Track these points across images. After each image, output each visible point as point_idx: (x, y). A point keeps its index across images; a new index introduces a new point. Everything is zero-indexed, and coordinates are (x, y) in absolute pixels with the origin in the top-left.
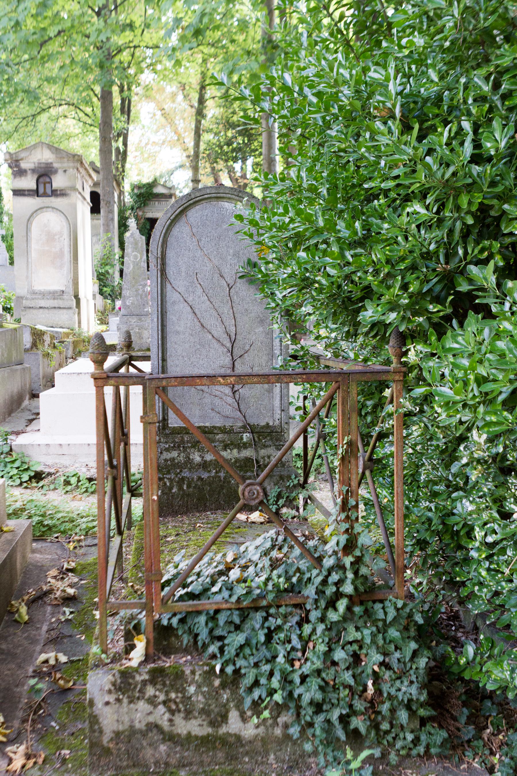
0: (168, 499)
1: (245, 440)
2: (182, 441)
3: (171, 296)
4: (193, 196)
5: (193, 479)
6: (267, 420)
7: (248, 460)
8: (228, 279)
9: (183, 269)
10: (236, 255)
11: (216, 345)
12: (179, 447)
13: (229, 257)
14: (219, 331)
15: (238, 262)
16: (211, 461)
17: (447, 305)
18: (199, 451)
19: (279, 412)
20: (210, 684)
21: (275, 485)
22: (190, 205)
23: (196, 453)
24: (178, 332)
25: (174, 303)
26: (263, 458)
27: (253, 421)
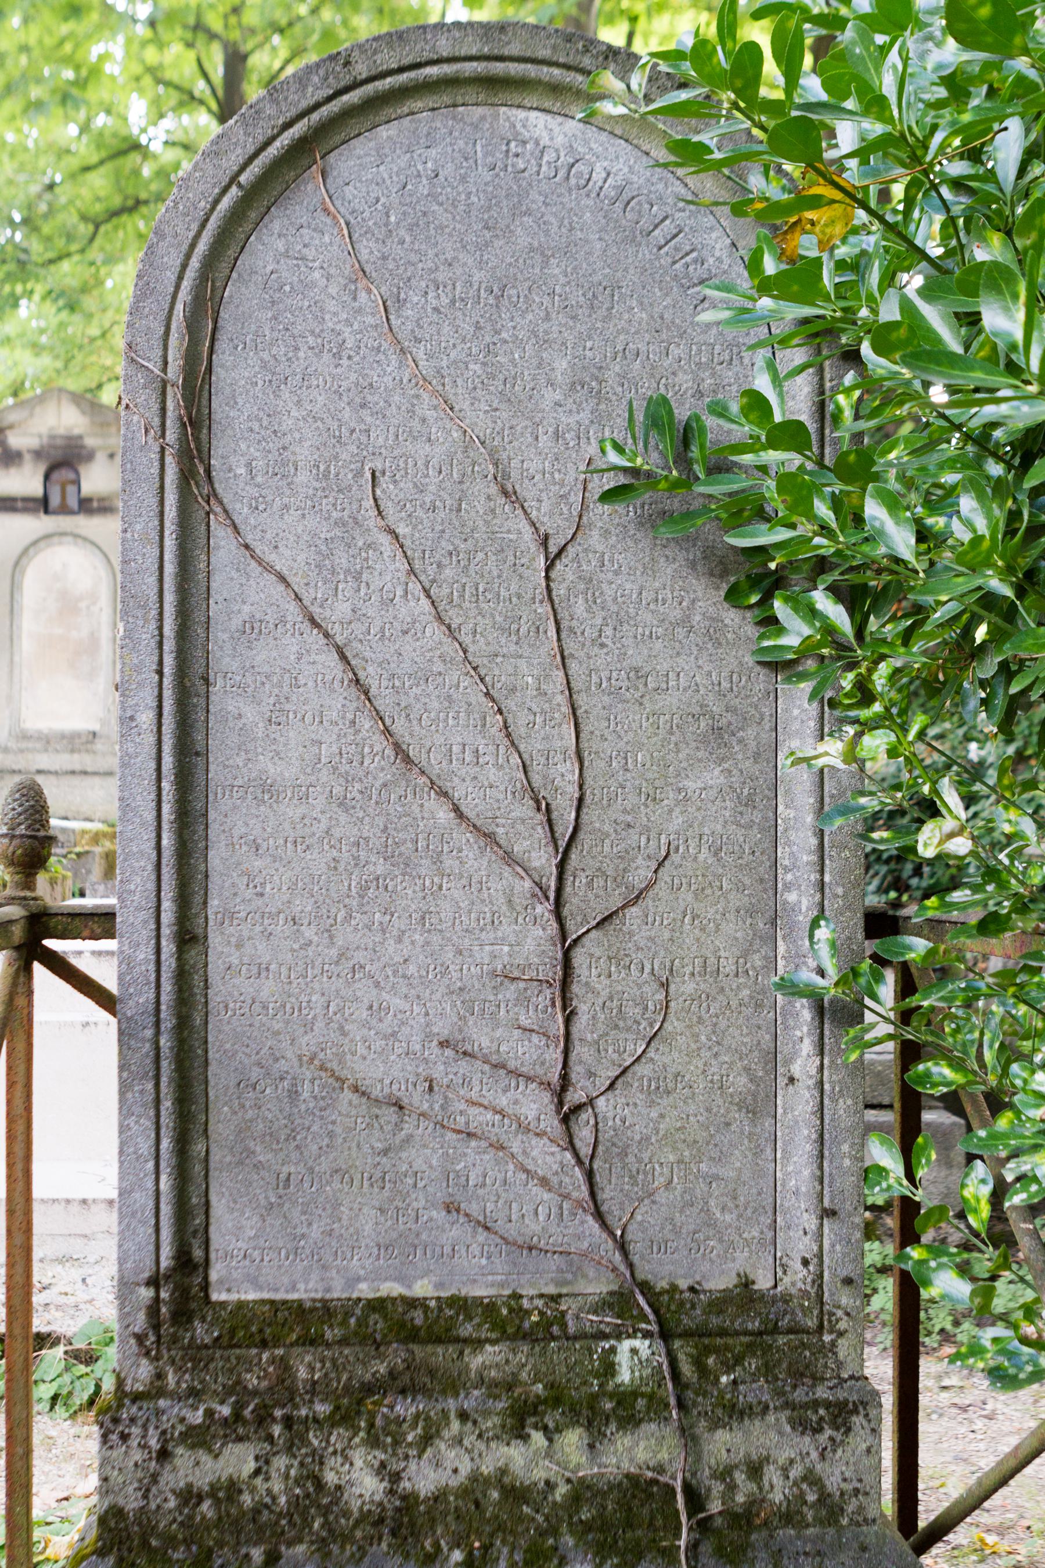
1: (624, 1376)
3: (236, 592)
4: (362, 69)
6: (740, 1261)
7: (641, 1491)
8: (543, 511)
10: (587, 384)
11: (475, 859)
12: (263, 1418)
13: (551, 396)
14: (488, 785)
15: (599, 419)
16: (439, 1497)
18: (373, 1442)
19: (810, 1222)
23: (359, 1457)
25: (251, 629)
26: (724, 1474)
27: (663, 1269)
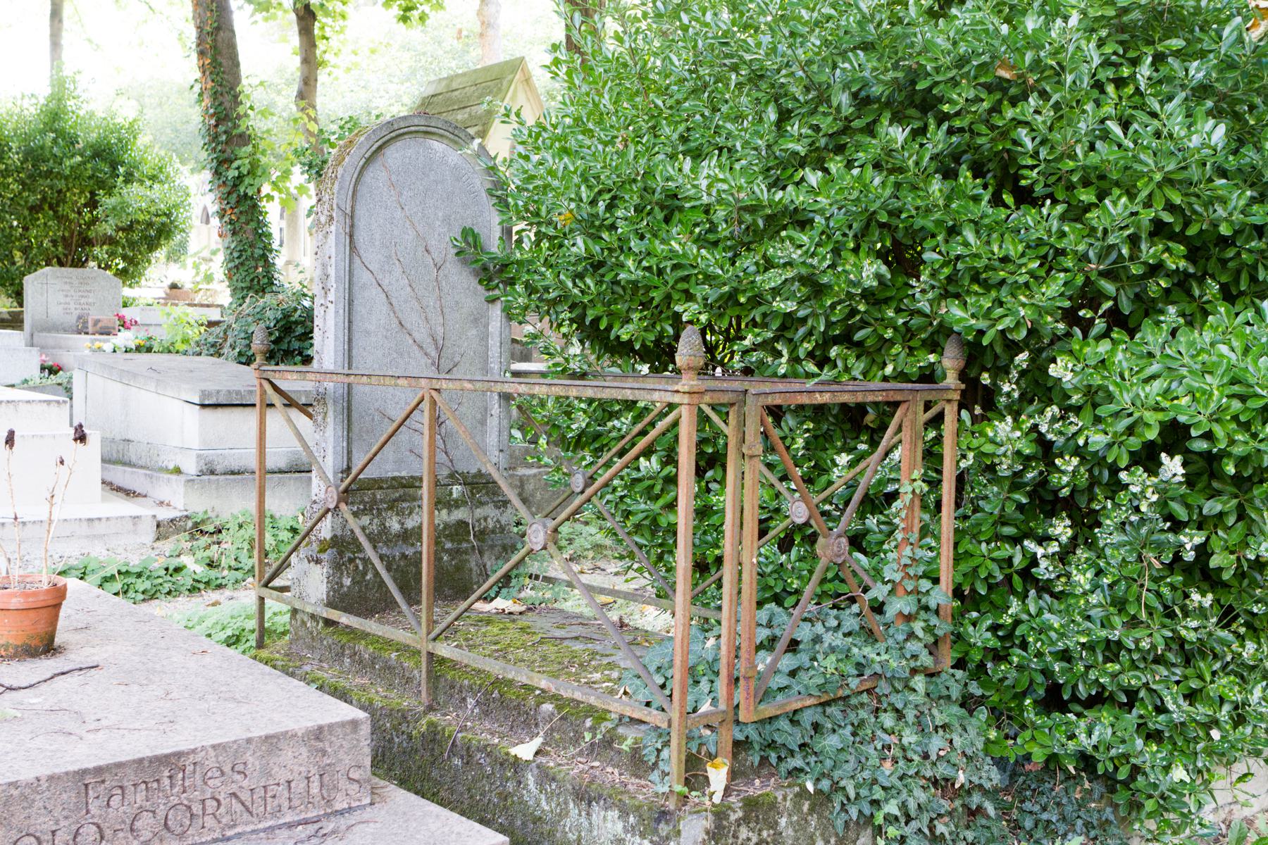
0: (360, 591)
1: (455, 496)
2: (374, 501)
3: (363, 277)
4: (396, 126)
5: (394, 557)
6: (479, 465)
7: (462, 524)
8: (435, 255)
9: (377, 236)
10: (446, 220)
11: (417, 353)
12: (371, 509)
13: (438, 223)
14: (421, 334)
15: (449, 230)
16: (413, 528)
17: (1100, 312)
18: (398, 514)
19: (497, 453)
20: (800, 810)
21: (497, 559)
22: (392, 138)
23: (394, 518)
24: (368, 333)
25: (364, 287)
26: (478, 521)
27: (462, 467)
